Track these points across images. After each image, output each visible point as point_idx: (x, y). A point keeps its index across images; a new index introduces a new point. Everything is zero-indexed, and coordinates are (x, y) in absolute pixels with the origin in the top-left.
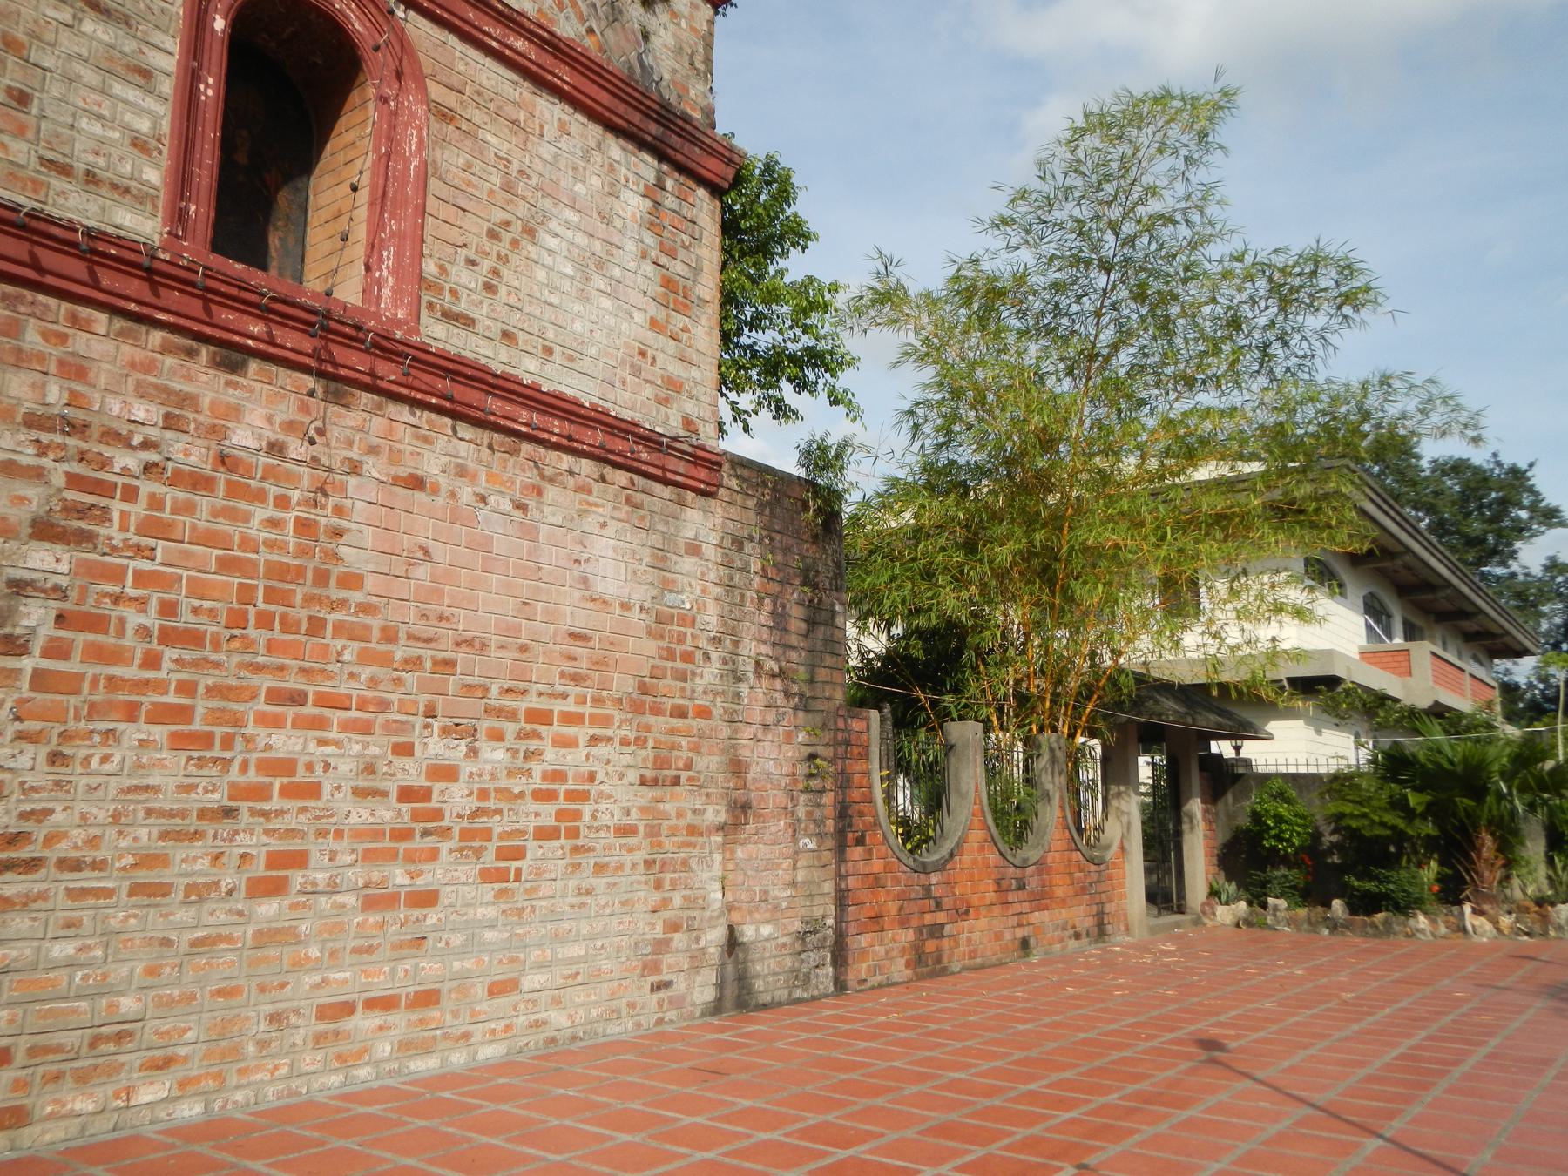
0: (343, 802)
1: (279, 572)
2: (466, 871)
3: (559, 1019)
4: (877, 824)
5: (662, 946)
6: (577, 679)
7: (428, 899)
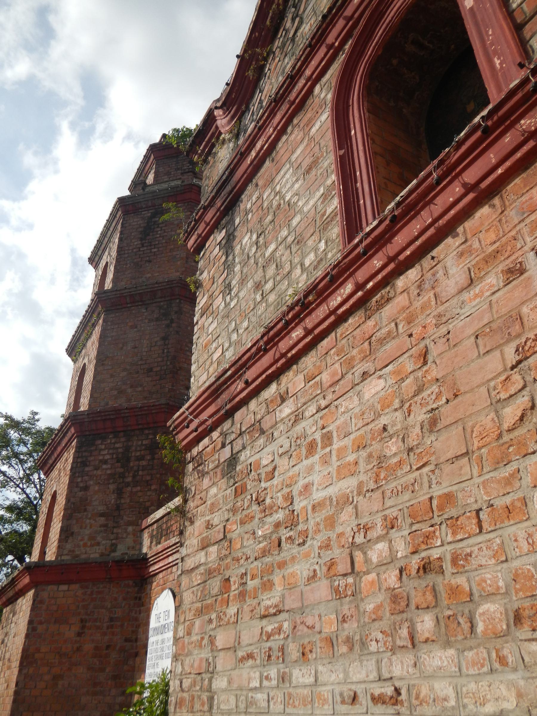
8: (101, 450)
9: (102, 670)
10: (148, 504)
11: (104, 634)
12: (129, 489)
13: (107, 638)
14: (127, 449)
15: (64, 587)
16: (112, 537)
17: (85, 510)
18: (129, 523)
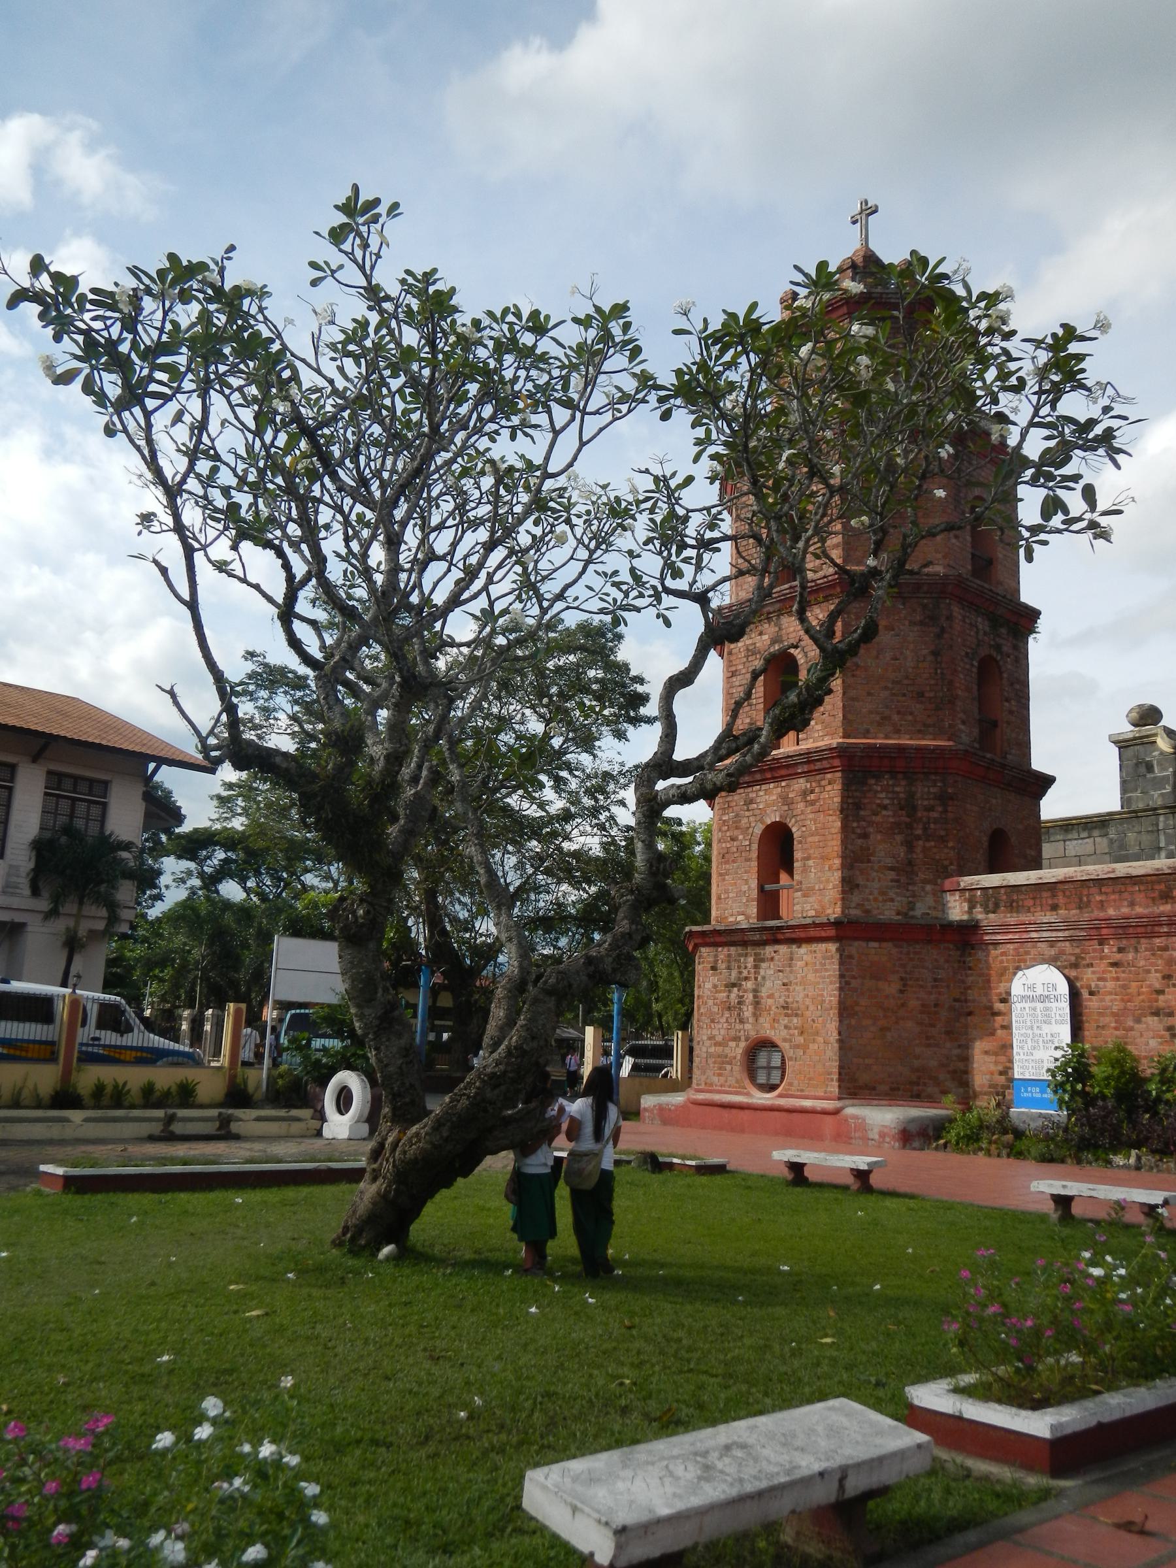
8: (877, 792)
9: (933, 1026)
10: (946, 863)
11: (930, 993)
12: (921, 843)
13: (933, 997)
14: (911, 795)
16: (908, 894)
17: (869, 861)
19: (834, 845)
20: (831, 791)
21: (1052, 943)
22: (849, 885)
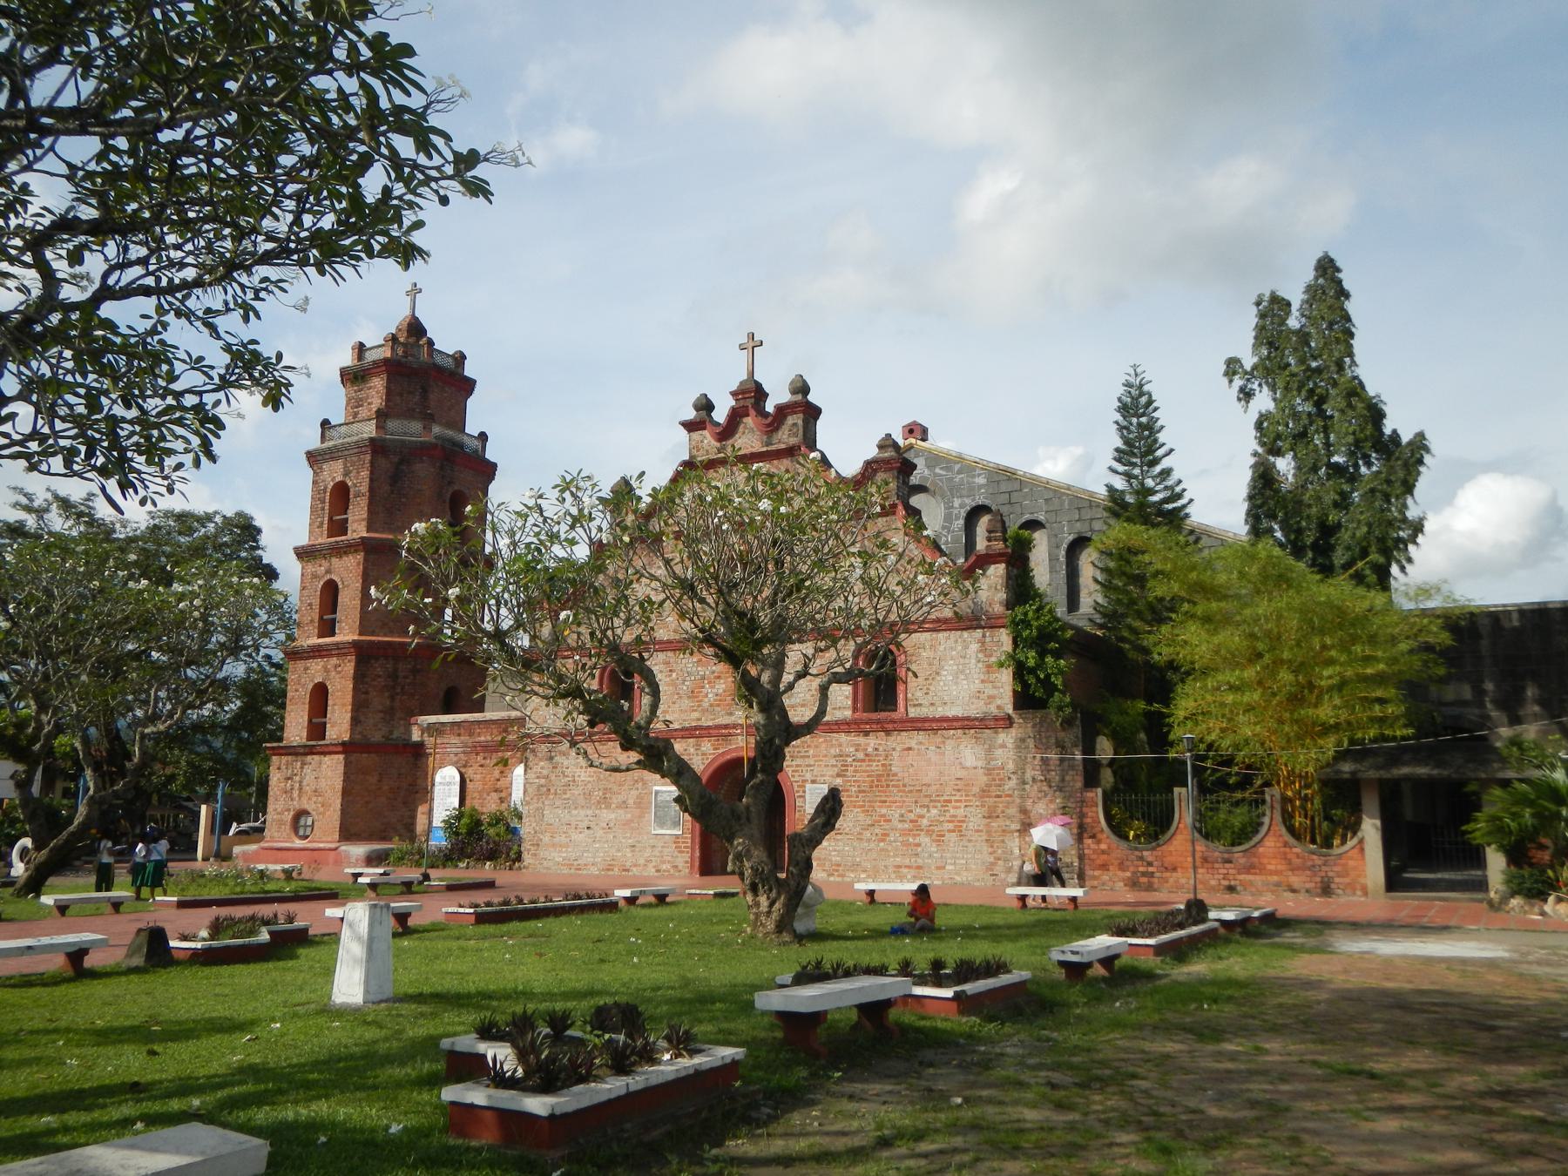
0: (895, 823)
1: (879, 775)
2: (927, 840)
3: (958, 878)
4: (1102, 831)
5: (992, 864)
6: (959, 790)
7: (919, 845)
15: (365, 755)
18: (401, 719)
19: (349, 698)
20: (349, 667)
21: (456, 754)
22: (355, 721)
